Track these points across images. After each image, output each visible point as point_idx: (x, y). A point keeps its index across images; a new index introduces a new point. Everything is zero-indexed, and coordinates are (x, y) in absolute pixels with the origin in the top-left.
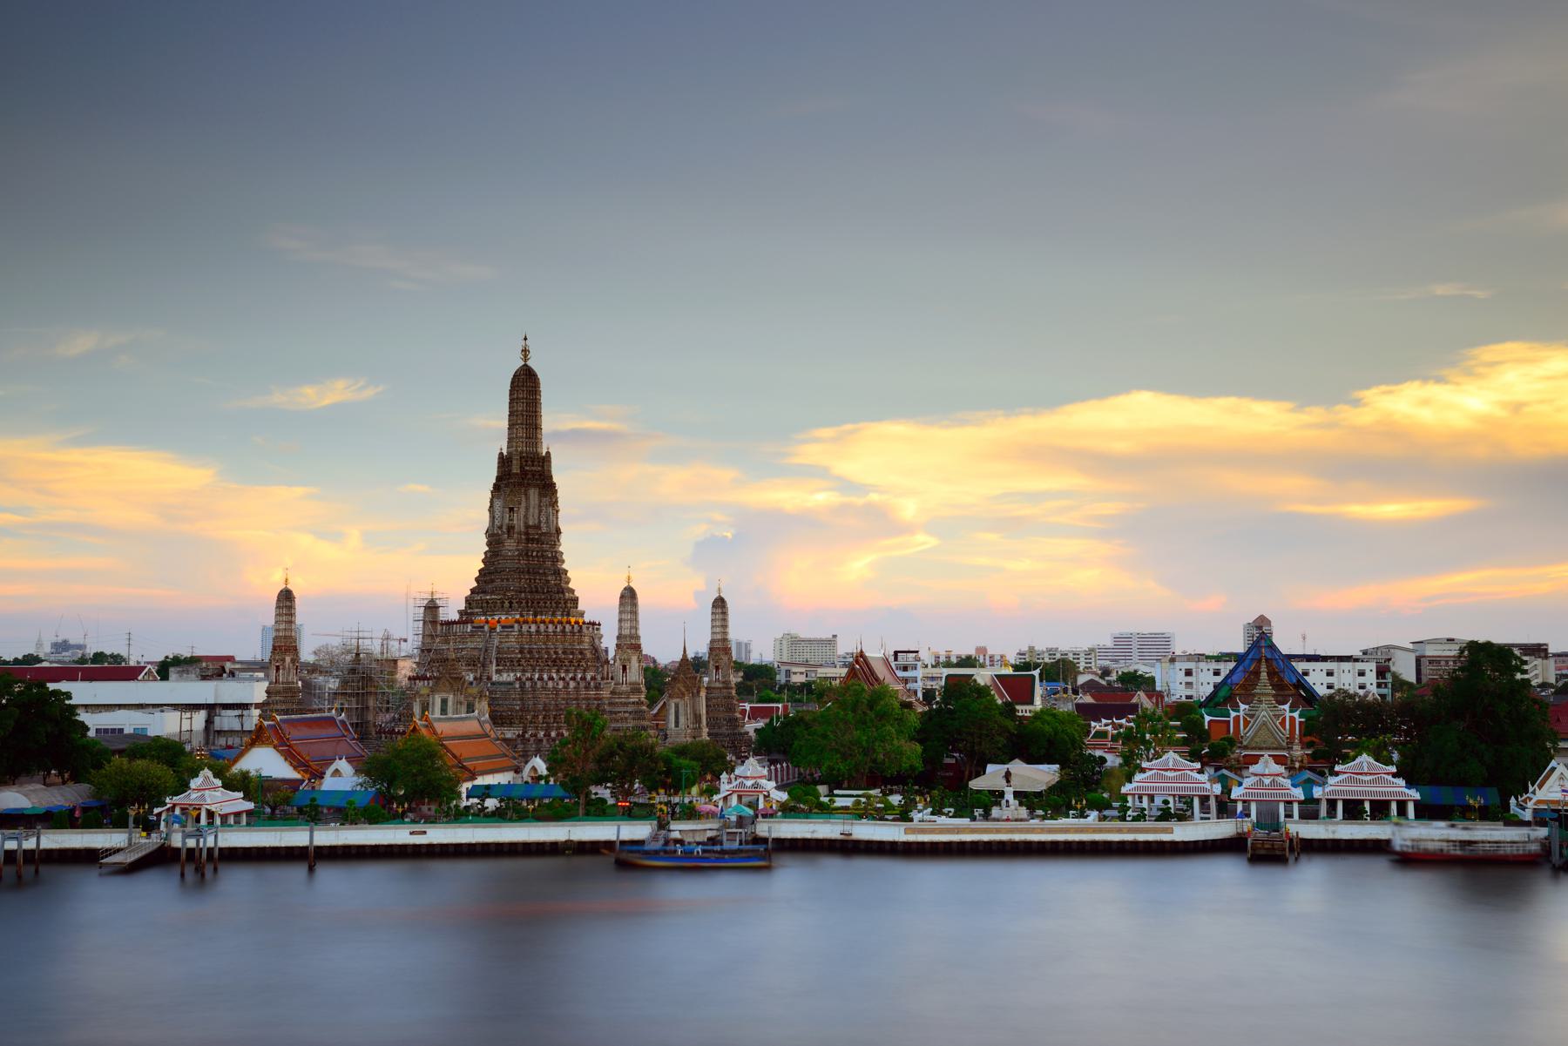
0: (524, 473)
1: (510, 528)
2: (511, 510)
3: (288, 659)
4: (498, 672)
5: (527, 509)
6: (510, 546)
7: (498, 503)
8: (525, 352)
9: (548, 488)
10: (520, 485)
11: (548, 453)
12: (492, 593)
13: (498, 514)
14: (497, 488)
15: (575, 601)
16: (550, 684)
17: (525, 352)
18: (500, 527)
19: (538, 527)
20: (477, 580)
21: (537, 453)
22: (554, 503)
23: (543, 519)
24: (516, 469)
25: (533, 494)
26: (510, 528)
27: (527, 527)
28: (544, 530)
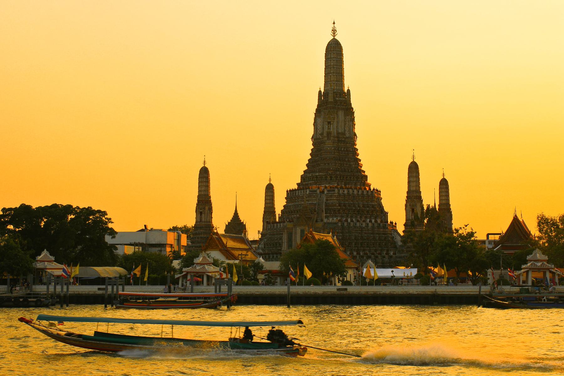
0: (336, 102)
1: (329, 134)
2: (329, 123)
3: (207, 208)
4: (326, 217)
5: (338, 122)
6: (329, 145)
7: (319, 120)
8: (334, 31)
9: (349, 112)
11: (349, 91)
12: (319, 172)
13: (319, 127)
15: (366, 177)
16: (358, 224)
17: (334, 31)
18: (322, 134)
19: (344, 134)
20: (307, 165)
21: (342, 91)
22: (353, 120)
23: (347, 129)
24: (331, 99)
25: (341, 114)
26: (329, 134)
27: (338, 133)
28: (347, 135)
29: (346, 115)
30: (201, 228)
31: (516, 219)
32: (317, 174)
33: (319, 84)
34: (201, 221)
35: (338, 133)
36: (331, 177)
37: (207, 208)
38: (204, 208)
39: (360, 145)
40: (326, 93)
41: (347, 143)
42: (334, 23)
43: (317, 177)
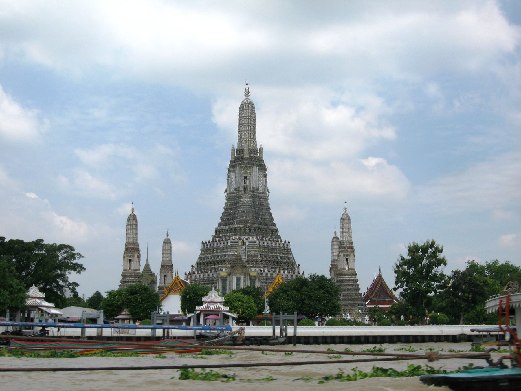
0: (251, 158)
1: (246, 188)
3: (136, 256)
9: (262, 168)
10: (249, 163)
11: (261, 148)
14: (232, 166)
18: (237, 189)
19: (258, 189)
23: (260, 184)
24: (246, 155)
25: (255, 169)
26: (246, 188)
27: (253, 188)
29: (260, 170)
30: (130, 275)
31: (380, 276)
32: (236, 226)
33: (234, 140)
34: (130, 268)
35: (253, 188)
36: (250, 229)
37: (136, 256)
38: (134, 256)
39: (272, 200)
40: (240, 151)
41: (261, 198)
42: (247, 85)
43: (235, 229)
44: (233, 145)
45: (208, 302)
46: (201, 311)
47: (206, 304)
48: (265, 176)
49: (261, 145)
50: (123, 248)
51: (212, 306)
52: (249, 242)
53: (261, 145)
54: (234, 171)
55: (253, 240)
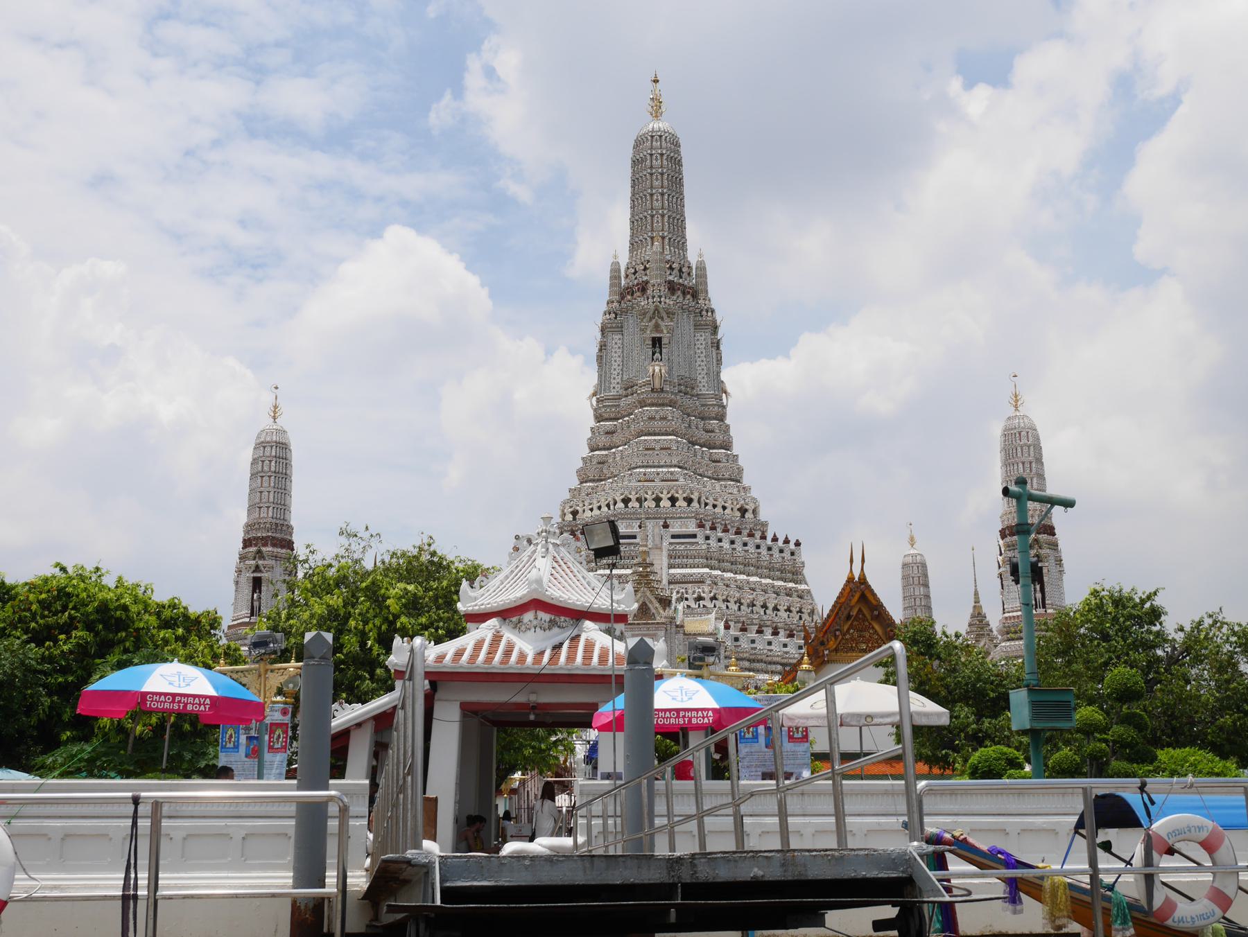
11: (702, 268)
44: (615, 257)
45: (506, 614)
46: (438, 680)
47: (485, 631)
48: (717, 345)
49: (701, 256)
50: (239, 536)
51: (526, 647)
52: (673, 537)
53: (701, 256)
54: (620, 329)
55: (684, 530)
